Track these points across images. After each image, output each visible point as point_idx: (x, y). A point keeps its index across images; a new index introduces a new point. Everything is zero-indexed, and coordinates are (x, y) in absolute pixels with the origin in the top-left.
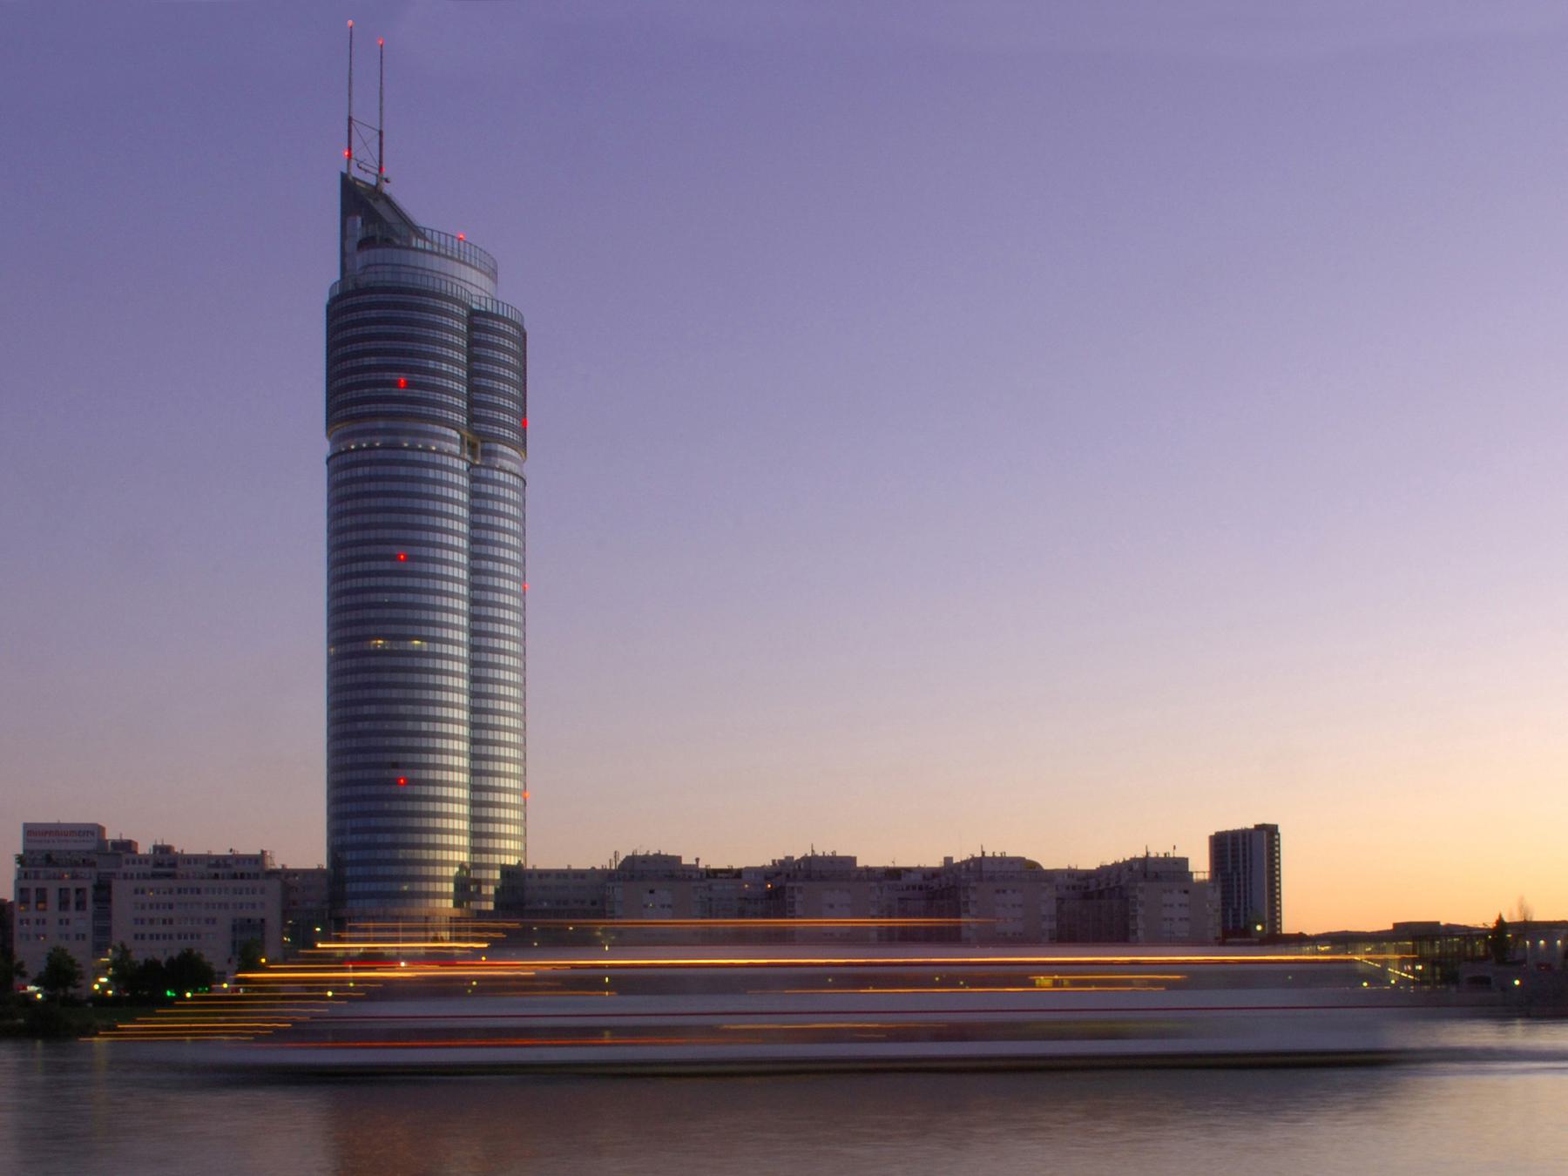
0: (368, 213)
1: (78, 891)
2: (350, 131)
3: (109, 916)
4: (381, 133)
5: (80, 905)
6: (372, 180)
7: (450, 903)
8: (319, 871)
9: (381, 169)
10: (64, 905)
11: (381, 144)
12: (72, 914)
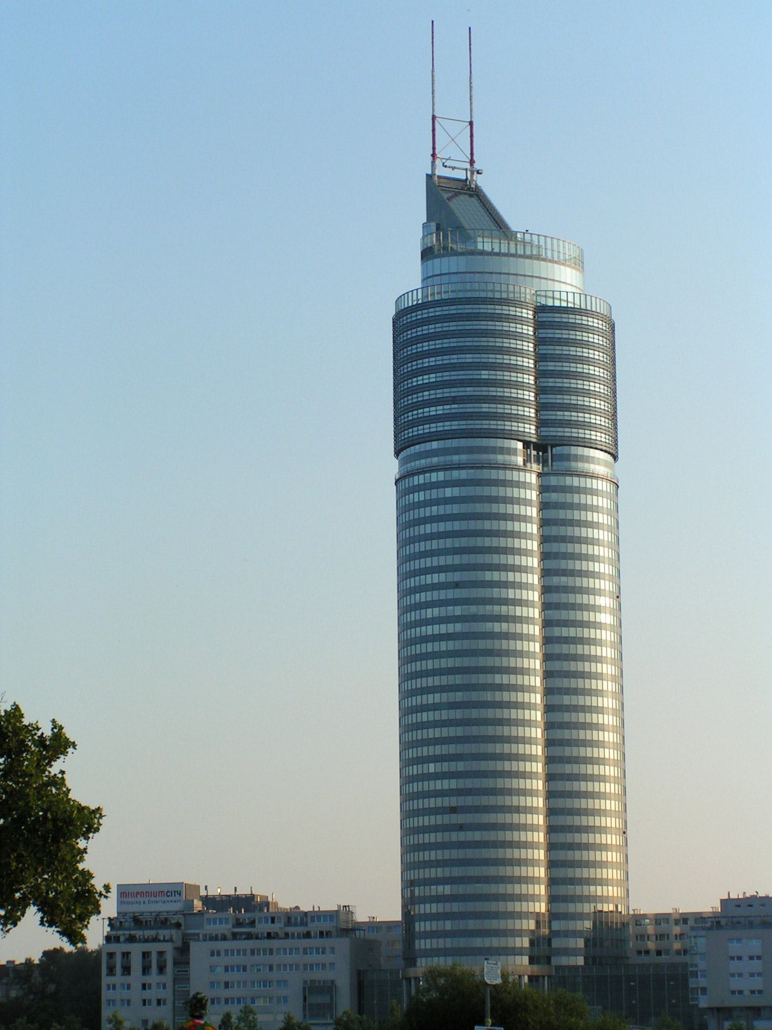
0: (456, 212)
1: (161, 954)
2: (434, 130)
3: (188, 980)
4: (471, 123)
5: (161, 969)
6: (461, 175)
7: (526, 960)
8: (390, 926)
9: (472, 162)
10: (146, 970)
11: (472, 136)
12: (154, 978)
